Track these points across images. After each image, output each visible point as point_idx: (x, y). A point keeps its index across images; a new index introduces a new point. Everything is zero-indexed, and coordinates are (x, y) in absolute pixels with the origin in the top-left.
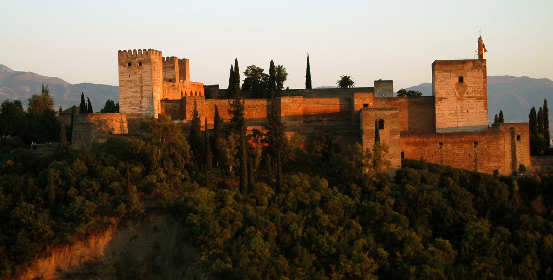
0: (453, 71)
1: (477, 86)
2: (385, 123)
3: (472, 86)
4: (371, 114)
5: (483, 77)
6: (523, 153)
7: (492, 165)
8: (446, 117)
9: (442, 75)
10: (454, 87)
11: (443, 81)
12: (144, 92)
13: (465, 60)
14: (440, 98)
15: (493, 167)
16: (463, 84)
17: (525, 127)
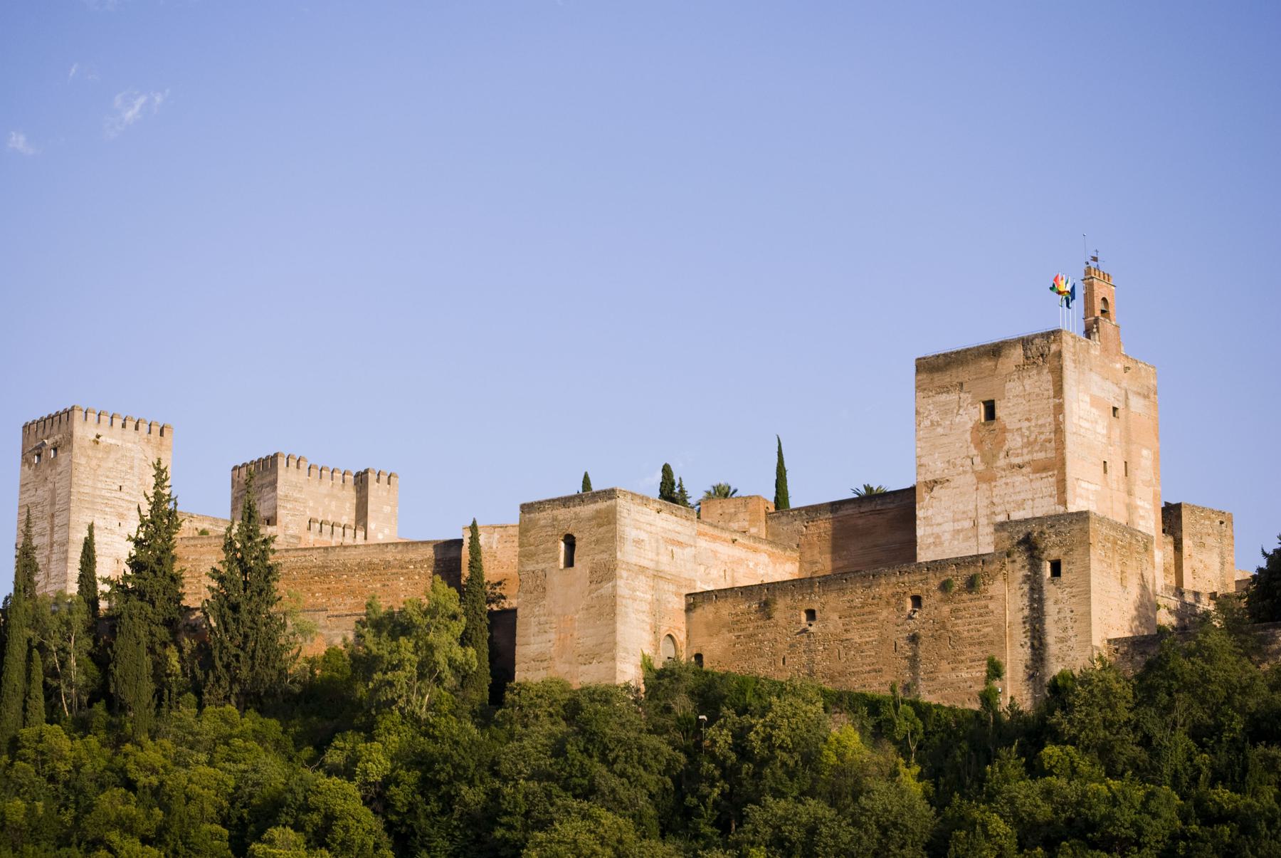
0: (965, 386)
1: (1036, 425)
2: (577, 544)
3: (1021, 428)
4: (542, 522)
5: (1051, 393)
6: (1070, 624)
7: (964, 675)
8: (946, 544)
9: (934, 403)
10: (969, 440)
11: (939, 425)
12: (56, 529)
13: (1002, 342)
14: (930, 481)
15: (969, 683)
16: (995, 425)
17: (1077, 527)
